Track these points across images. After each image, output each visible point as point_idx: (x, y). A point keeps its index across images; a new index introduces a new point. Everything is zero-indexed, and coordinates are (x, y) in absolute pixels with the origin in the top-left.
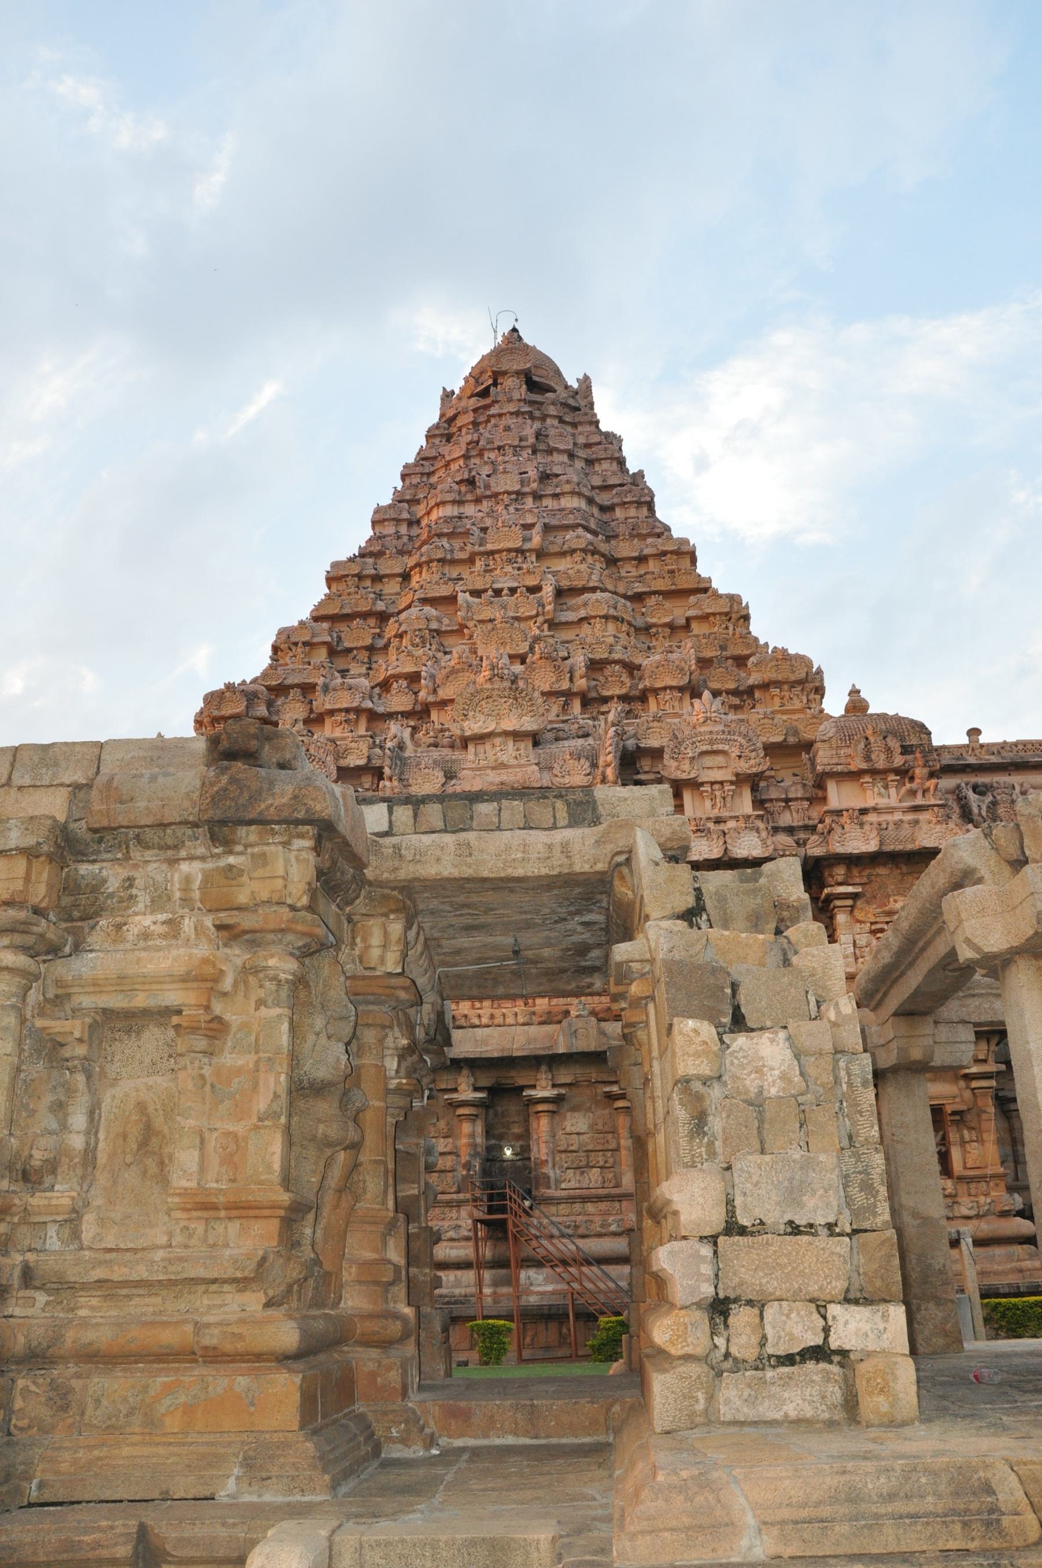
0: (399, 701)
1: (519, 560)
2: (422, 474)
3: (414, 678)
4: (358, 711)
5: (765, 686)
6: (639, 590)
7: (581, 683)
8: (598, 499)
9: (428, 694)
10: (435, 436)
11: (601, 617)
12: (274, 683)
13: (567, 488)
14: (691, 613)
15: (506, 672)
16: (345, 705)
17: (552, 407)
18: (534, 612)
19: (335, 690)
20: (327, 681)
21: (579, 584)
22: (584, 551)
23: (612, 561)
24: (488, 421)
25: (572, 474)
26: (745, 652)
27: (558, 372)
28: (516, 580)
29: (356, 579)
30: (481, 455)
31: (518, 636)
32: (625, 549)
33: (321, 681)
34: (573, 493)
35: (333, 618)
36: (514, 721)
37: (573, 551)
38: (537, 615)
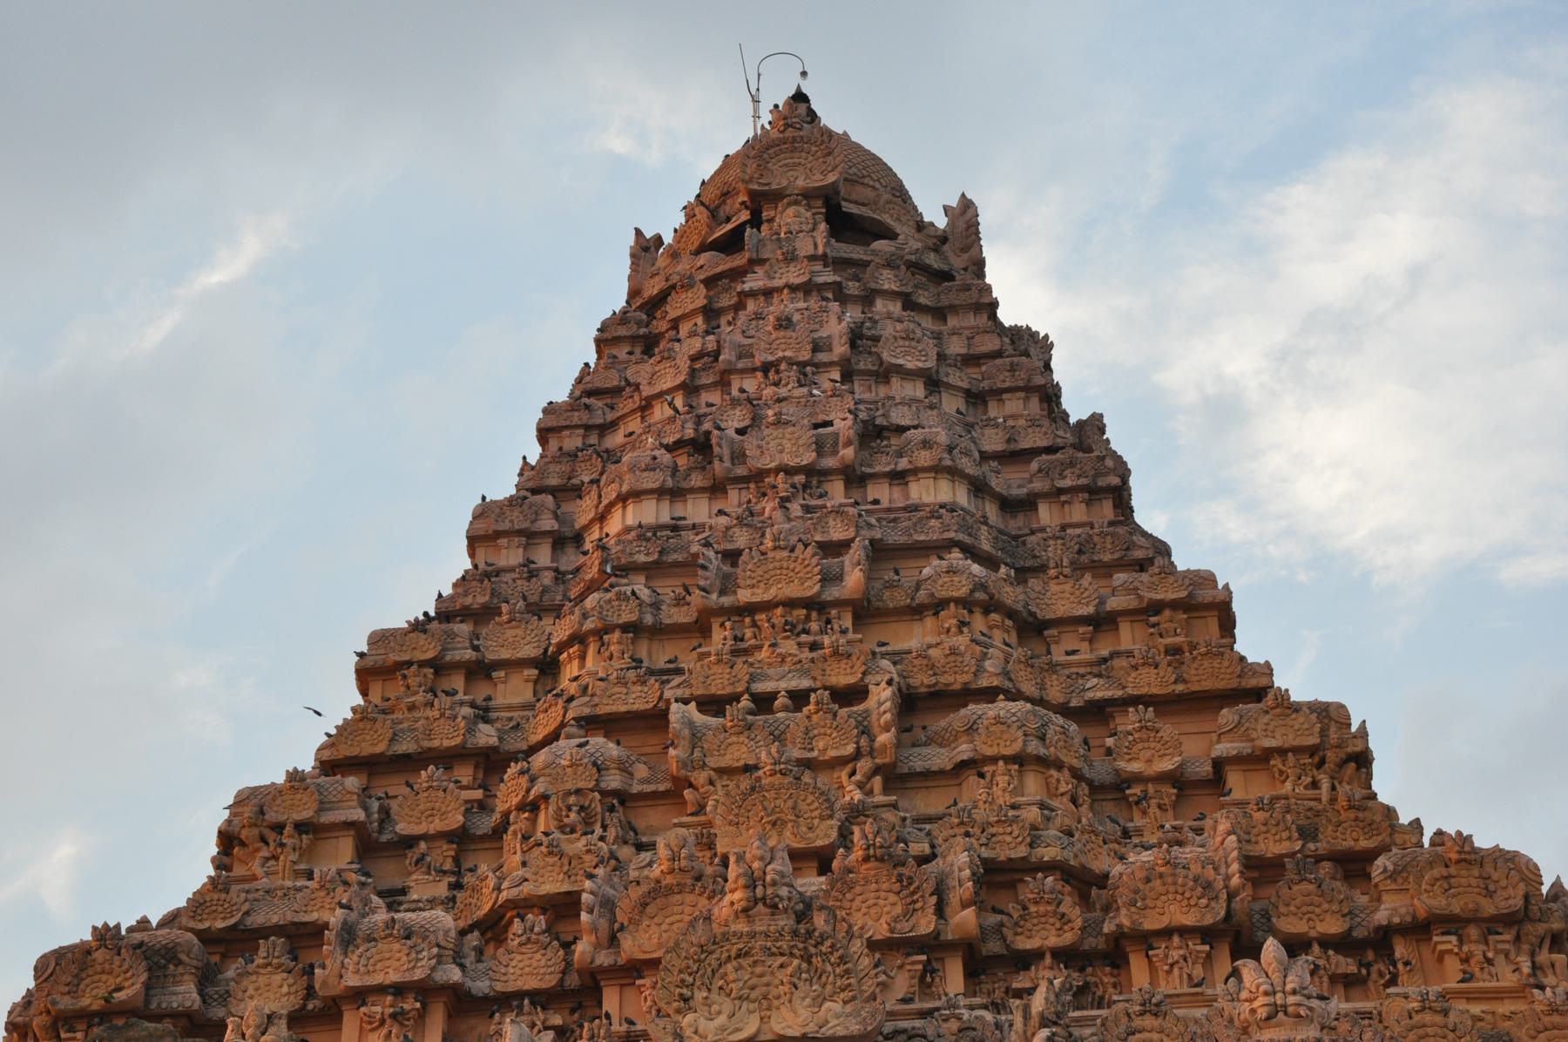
0: (525, 965)
1: (814, 626)
2: (588, 428)
3: (563, 908)
4: (425, 991)
5: (1420, 929)
6: (1099, 695)
7: (965, 919)
8: (996, 483)
9: (597, 946)
10: (616, 340)
11: (1009, 759)
12: (220, 924)
13: (924, 458)
14: (1224, 748)
15: (784, 891)
16: (393, 977)
17: (887, 273)
18: (850, 749)
19: (370, 939)
20: (353, 916)
21: (955, 681)
22: (966, 603)
23: (1031, 628)
24: (739, 306)
25: (933, 424)
26: (1365, 844)
27: (900, 193)
28: (806, 673)
29: (429, 671)
30: (723, 383)
31: (810, 805)
32: (1062, 598)
33: (335, 918)
34: (937, 470)
35: (372, 766)
36: (804, 1014)
37: (938, 606)
38: (857, 755)
